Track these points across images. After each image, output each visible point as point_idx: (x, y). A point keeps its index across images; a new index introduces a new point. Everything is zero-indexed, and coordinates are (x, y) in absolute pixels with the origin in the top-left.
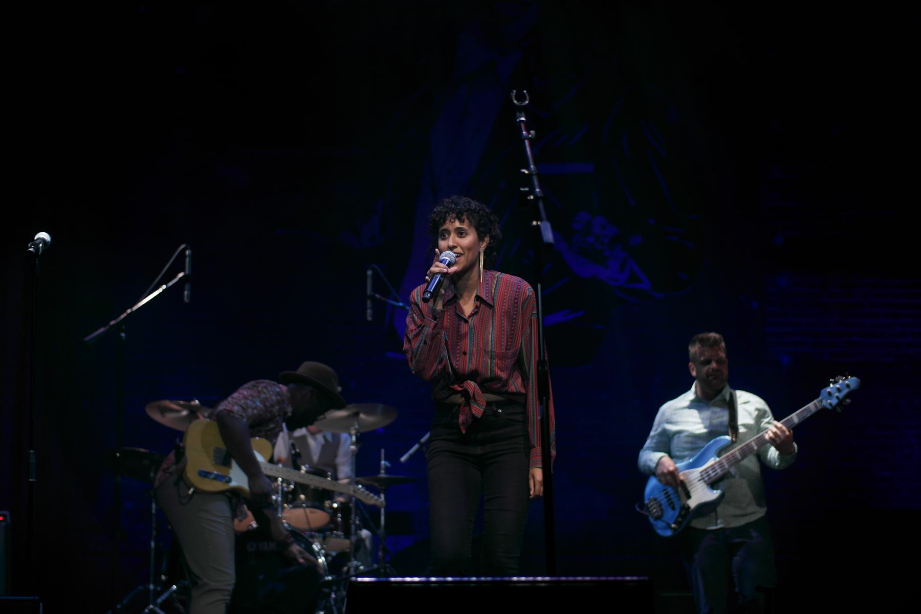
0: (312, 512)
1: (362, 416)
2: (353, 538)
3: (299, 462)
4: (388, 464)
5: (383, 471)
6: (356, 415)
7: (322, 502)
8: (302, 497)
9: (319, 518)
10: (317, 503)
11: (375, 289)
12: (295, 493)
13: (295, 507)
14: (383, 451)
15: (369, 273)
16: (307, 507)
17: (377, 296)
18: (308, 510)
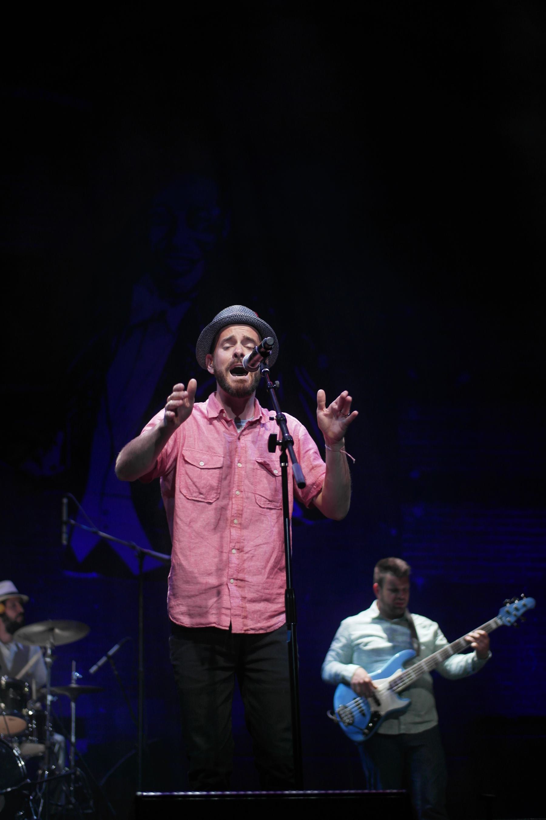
0: (10, 720)
1: (57, 631)
5: (73, 681)
6: (51, 630)
7: (20, 710)
10: (16, 711)
11: (70, 516)
14: (74, 664)
15: (65, 501)
16: (7, 715)
17: (73, 522)
18: (7, 718)
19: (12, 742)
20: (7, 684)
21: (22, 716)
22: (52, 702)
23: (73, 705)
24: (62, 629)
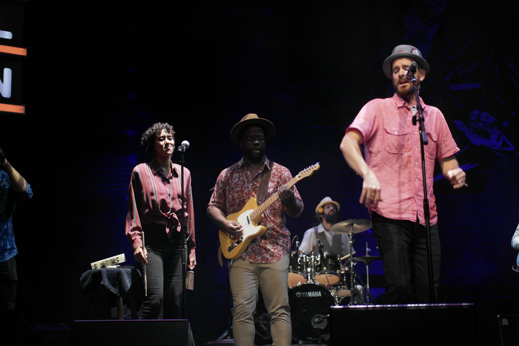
2: (352, 289)
3: (322, 250)
4: (369, 250)
8: (325, 268)
9: (334, 279)
12: (320, 266)
13: (321, 274)
18: (328, 275)
19: (331, 289)
20: (327, 256)
21: (336, 274)
22: (353, 265)
23: (367, 267)
24: (358, 224)
